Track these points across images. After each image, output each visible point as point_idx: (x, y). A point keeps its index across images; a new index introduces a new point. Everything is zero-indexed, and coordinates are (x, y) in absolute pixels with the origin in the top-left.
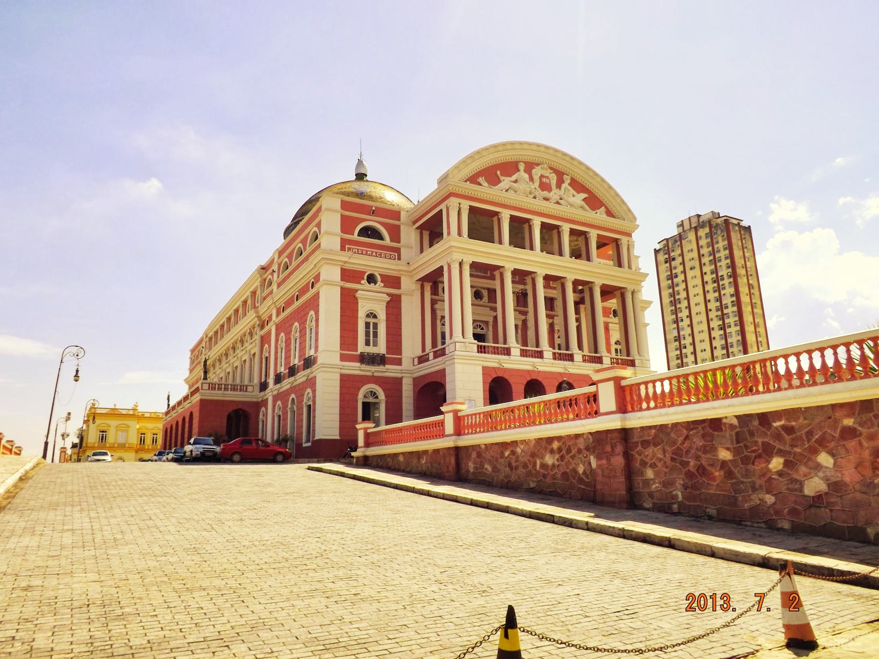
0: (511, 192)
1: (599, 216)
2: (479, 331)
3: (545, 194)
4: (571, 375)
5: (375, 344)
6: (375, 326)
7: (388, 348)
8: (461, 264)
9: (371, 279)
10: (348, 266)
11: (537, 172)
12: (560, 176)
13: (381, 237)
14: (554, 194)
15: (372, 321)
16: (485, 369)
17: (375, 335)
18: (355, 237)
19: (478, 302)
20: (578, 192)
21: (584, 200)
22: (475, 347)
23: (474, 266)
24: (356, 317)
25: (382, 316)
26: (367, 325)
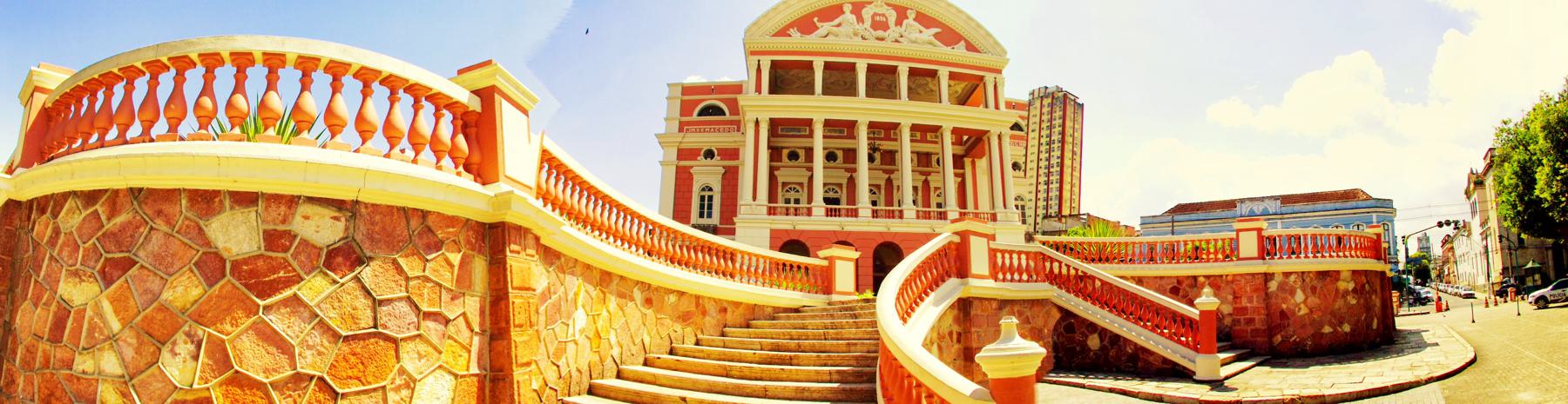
0: (830, 38)
1: (958, 53)
2: (831, 195)
3: (880, 33)
4: (802, 232)
5: (710, 216)
6: (711, 198)
7: (722, 217)
8: (757, 122)
9: (709, 154)
10: (684, 146)
11: (867, 13)
12: (902, 13)
13: (722, 112)
14: (893, 31)
15: (707, 194)
16: (772, 231)
17: (710, 207)
18: (695, 117)
19: (832, 164)
20: (927, 27)
21: (936, 36)
22: (765, 210)
23: (774, 124)
24: (690, 192)
25: (717, 188)
26: (702, 198)
